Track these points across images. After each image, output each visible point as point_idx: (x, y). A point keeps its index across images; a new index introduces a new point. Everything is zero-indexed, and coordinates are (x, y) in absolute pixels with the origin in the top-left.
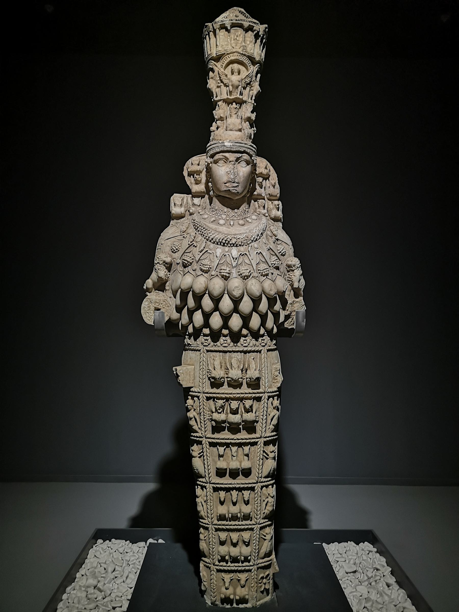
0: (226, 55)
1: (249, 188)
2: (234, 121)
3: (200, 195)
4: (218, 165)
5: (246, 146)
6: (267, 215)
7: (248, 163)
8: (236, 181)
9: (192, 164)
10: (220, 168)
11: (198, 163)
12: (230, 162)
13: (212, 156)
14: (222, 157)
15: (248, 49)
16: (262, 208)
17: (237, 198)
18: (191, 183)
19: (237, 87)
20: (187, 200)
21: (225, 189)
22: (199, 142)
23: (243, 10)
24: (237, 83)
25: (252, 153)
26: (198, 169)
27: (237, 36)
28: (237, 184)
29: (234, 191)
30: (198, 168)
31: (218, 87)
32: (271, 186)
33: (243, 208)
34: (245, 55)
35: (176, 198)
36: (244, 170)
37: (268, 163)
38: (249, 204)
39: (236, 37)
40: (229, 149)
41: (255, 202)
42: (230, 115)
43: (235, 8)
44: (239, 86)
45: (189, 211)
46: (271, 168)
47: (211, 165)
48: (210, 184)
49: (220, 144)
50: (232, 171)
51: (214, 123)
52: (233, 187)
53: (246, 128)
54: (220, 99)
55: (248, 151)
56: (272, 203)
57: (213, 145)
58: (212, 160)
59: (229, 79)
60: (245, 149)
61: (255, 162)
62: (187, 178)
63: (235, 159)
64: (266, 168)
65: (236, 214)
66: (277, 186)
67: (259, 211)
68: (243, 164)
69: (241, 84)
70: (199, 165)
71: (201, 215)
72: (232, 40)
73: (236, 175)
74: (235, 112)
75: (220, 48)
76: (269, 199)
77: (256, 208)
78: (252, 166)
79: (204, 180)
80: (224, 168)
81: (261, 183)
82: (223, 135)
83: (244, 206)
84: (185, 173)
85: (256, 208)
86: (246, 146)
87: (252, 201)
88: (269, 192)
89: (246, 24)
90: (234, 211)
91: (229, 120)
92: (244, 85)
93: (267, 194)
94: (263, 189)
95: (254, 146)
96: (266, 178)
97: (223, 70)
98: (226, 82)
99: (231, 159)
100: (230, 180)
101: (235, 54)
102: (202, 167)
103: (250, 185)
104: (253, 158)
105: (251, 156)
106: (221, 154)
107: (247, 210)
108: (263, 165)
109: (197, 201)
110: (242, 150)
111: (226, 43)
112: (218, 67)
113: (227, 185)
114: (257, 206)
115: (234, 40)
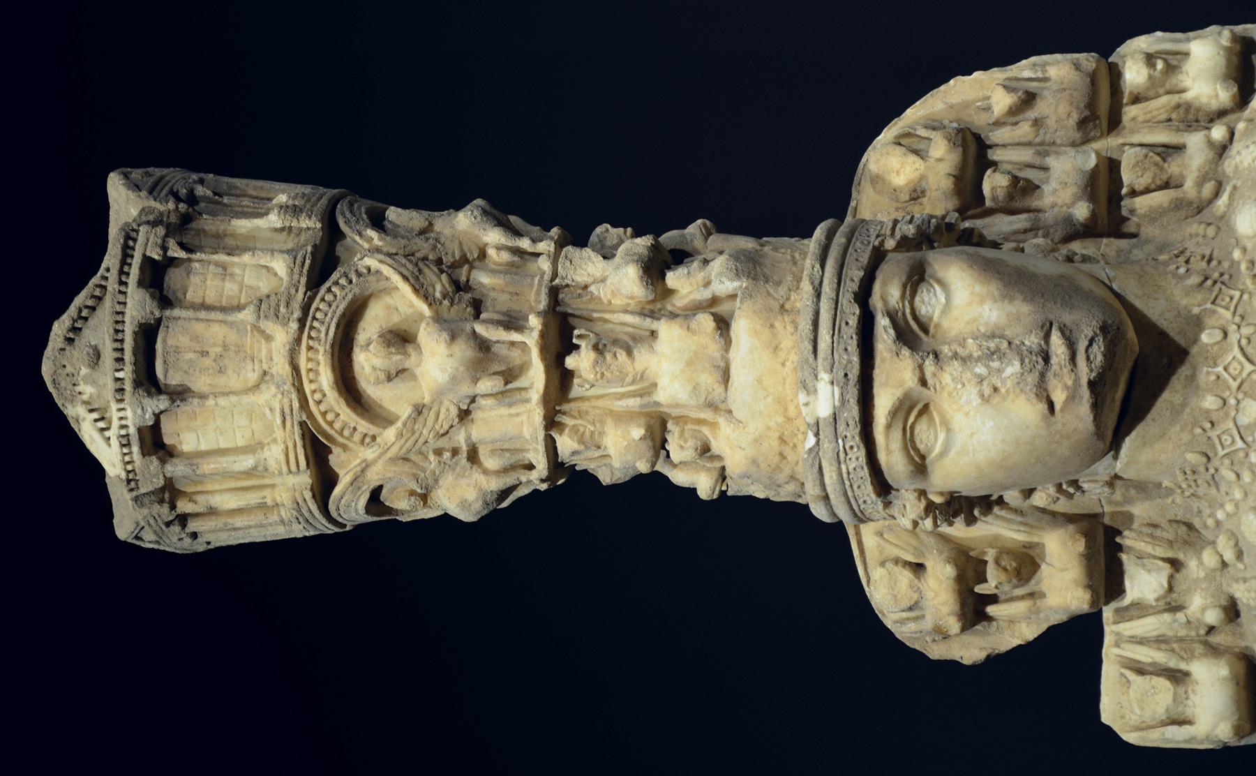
0: (310, 415)
2: (670, 364)
4: (943, 454)
5: (827, 289)
8: (1033, 341)
10: (959, 441)
11: (905, 576)
12: (924, 382)
13: (883, 487)
14: (897, 434)
15: (265, 286)
16: (1173, 167)
19: (484, 346)
20: (1141, 641)
21: (1084, 409)
22: (780, 558)
23: (59, 328)
24: (463, 350)
27: (204, 354)
29: (1098, 352)
30: (941, 575)
31: (473, 456)
33: (1188, 292)
34: (306, 309)
35: (1129, 705)
36: (962, 299)
39: (208, 362)
42: (633, 382)
43: (46, 370)
44: (474, 334)
45: (1211, 629)
46: (914, 114)
47: (938, 500)
49: (827, 446)
51: (679, 478)
52: (1073, 359)
53: (707, 284)
54: (541, 447)
55: (855, 274)
56: (1136, 99)
59: (439, 394)
60: (847, 299)
63: (906, 352)
65: (1233, 338)
66: (1024, 69)
67: (1200, 183)
68: (930, 303)
69: (468, 327)
71: (1240, 555)
72: (221, 381)
73: (996, 346)
74: (622, 356)
75: (274, 455)
76: (1114, 123)
80: (958, 421)
82: (755, 427)
84: (970, 650)
85: (1178, 205)
86: (827, 289)
89: (138, 305)
91: (672, 390)
92: (463, 308)
93: (1078, 136)
97: (390, 434)
98: (454, 411)
100: (1032, 379)
101: (303, 365)
105: (879, 256)
110: (852, 313)
111: (241, 420)
112: (366, 462)
113: (1059, 397)
114: (1159, 198)
115: (221, 371)
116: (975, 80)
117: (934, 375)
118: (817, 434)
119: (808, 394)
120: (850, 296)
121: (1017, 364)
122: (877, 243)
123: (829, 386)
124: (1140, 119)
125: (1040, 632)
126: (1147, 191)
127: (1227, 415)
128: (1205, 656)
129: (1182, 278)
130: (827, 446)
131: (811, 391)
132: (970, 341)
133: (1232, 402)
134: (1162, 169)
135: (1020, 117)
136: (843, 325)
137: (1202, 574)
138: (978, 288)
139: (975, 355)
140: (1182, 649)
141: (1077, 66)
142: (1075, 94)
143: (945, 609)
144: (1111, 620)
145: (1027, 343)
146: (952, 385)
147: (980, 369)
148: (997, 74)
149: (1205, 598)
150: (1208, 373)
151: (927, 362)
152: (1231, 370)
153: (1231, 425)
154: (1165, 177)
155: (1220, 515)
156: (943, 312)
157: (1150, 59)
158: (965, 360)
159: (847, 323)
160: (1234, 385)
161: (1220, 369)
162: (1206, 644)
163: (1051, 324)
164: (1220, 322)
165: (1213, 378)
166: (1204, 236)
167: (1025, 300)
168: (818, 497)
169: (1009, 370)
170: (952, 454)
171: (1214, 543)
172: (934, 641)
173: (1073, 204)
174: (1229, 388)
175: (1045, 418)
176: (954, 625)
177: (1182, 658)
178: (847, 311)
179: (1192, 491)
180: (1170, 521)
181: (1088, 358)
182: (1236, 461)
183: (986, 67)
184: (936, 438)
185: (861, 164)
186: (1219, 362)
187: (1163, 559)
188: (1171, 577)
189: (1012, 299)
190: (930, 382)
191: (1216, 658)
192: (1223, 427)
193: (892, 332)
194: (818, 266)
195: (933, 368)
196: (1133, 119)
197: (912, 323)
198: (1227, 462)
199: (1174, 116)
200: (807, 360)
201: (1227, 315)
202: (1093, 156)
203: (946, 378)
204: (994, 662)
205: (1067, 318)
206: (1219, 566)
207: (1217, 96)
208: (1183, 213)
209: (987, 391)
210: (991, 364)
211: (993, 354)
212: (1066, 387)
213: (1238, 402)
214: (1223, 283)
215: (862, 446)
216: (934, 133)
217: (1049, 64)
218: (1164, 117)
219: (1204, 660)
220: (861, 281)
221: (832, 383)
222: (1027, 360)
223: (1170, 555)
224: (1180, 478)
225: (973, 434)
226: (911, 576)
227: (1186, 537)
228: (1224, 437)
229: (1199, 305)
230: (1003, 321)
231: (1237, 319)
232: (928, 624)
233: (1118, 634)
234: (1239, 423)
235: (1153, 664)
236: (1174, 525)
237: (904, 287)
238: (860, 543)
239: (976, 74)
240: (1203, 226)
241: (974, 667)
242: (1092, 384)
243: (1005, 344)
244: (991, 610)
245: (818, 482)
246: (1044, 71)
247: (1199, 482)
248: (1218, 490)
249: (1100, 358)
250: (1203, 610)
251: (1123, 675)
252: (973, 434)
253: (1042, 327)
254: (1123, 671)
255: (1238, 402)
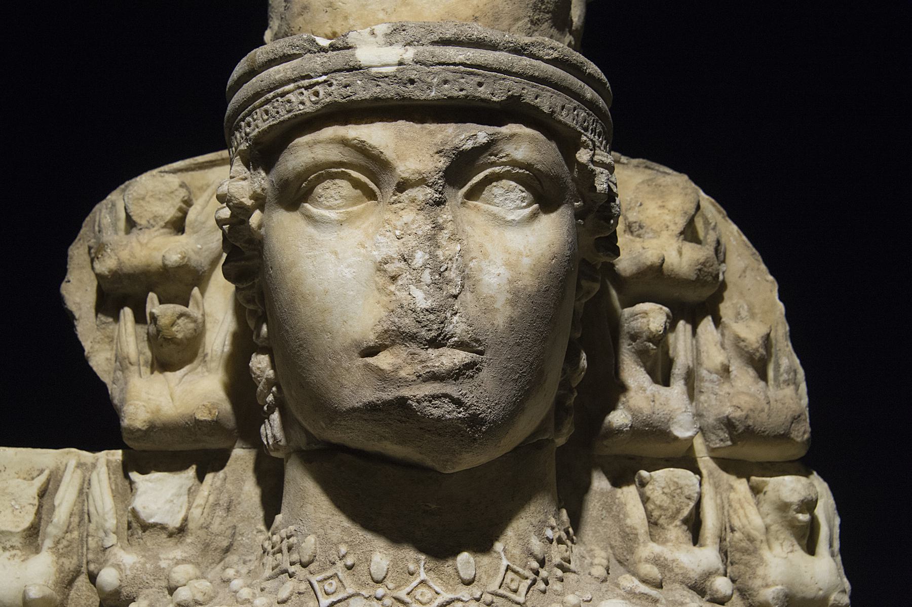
1: (565, 385)
3: (187, 448)
4: (311, 219)
5: (524, 63)
6: (722, 585)
7: (544, 192)
8: (457, 326)
9: (131, 224)
10: (327, 237)
11: (169, 211)
12: (402, 186)
14: (334, 154)
16: (676, 532)
17: (470, 460)
18: (122, 363)
20: (84, 493)
21: (369, 395)
25: (570, 116)
26: (174, 258)
28: (461, 357)
29: (445, 410)
32: (732, 359)
33: (522, 538)
36: (510, 246)
37: (706, 200)
38: (573, 502)
40: (388, 90)
41: (617, 482)
45: (92, 578)
47: (255, 218)
48: (260, 363)
49: (316, 62)
50: (420, 258)
52: (435, 377)
56: (756, 490)
57: (275, 76)
58: (261, 181)
60: (514, 86)
61: (601, 185)
62: (88, 328)
63: (443, 163)
64: (689, 233)
65: (464, 593)
66: (787, 359)
67: (656, 561)
68: (509, 199)
70: (178, 226)
77: (629, 538)
78: (578, 215)
79: (219, 334)
80: (352, 236)
81: (660, 340)
83: (528, 531)
84: (79, 293)
85: (629, 538)
86: (524, 63)
87: (600, 483)
88: (728, 411)
90: (447, 567)
93: (711, 420)
94: (678, 388)
95: (592, 68)
96: (696, 299)
99: (406, 167)
100: (408, 324)
102: (202, 242)
103: (572, 358)
104: (583, 156)
105: (567, 142)
106: (329, 132)
107: (556, 554)
108: (660, 214)
109: (162, 494)
110: (494, 91)
113: (384, 360)
114: (636, 514)
116: (774, 305)
117: (413, 201)
118: (333, 48)
119: (386, 35)
120: (516, 90)
121: (427, 304)
122: (584, 138)
123: (396, 59)
124: (732, 495)
125: (99, 374)
126: (645, 500)
127: (363, 585)
128: (60, 570)
129: (540, 533)
130: (316, 62)
131: (390, 38)
132: (458, 248)
133: (380, 591)
134: (673, 517)
135: (732, 353)
136: (478, 79)
137: (163, 564)
138: (526, 262)
139: (439, 253)
140: (71, 542)
141: (796, 419)
142: (764, 415)
143: (125, 255)
144: (111, 458)
145: (456, 318)
146: (399, 224)
147: (420, 258)
148: (782, 331)
149: (131, 569)
150: (418, 561)
151: (429, 190)
152: (422, 589)
153: (350, 591)
154: (662, 521)
155: (236, 583)
156: (495, 217)
157: (809, 505)
158: (432, 239)
159: (480, 84)
160: (402, 594)
161: (423, 576)
162: (77, 573)
163: (481, 353)
164: (484, 577)
165: (412, 567)
166: (592, 564)
167: (512, 320)
168: (254, 61)
169: (419, 294)
170: (311, 230)
171: (203, 577)
172: (90, 248)
173: (630, 409)
174: (398, 587)
175: (357, 344)
176: (107, 265)
177: (58, 542)
178: (497, 86)
179: (269, 548)
180: (235, 527)
181: (435, 397)
182: (302, 598)
183: (789, 316)
184: (329, 208)
185: (670, 171)
186: (432, 574)
187: (185, 519)
188: (163, 527)
189: (513, 303)
190: (404, 196)
191: (56, 584)
192: (347, 582)
193: (469, 145)
194: (555, 55)
195: (421, 197)
196: (731, 488)
197: (481, 175)
198: (303, 587)
199: (737, 535)
200: (431, 32)
201: (494, 586)
202: (688, 434)
203: (409, 216)
204: (66, 320)
205: (485, 375)
206: (173, 584)
207: (767, 586)
208: (617, 542)
209: (391, 268)
210: (428, 271)
211: (440, 275)
212: (396, 370)
213: (379, 599)
214: (534, 582)
215: (319, 106)
216: (712, 249)
217: (797, 389)
218: (737, 523)
219: (53, 570)
220: (537, 108)
221: (400, 64)
222: (432, 317)
223: (191, 525)
224: (283, 533)
225: (336, 253)
226: (168, 218)
227: (214, 545)
228: (334, 582)
229: (505, 550)
230: (485, 291)
231: (488, 598)
232: (108, 236)
233: (94, 466)
234: (351, 601)
235: (53, 508)
236: (229, 532)
237: (528, 166)
238: (212, 164)
239: (781, 306)
240: (605, 562)
241: (59, 300)
242: (402, 402)
243: (455, 291)
244: (127, 313)
245: (271, 56)
246: (787, 383)
247: (279, 556)
248: (270, 578)
249: (436, 412)
250: (118, 566)
251: (42, 471)
252: (336, 253)
253: (477, 341)
254: (47, 472)
255: (379, 599)
